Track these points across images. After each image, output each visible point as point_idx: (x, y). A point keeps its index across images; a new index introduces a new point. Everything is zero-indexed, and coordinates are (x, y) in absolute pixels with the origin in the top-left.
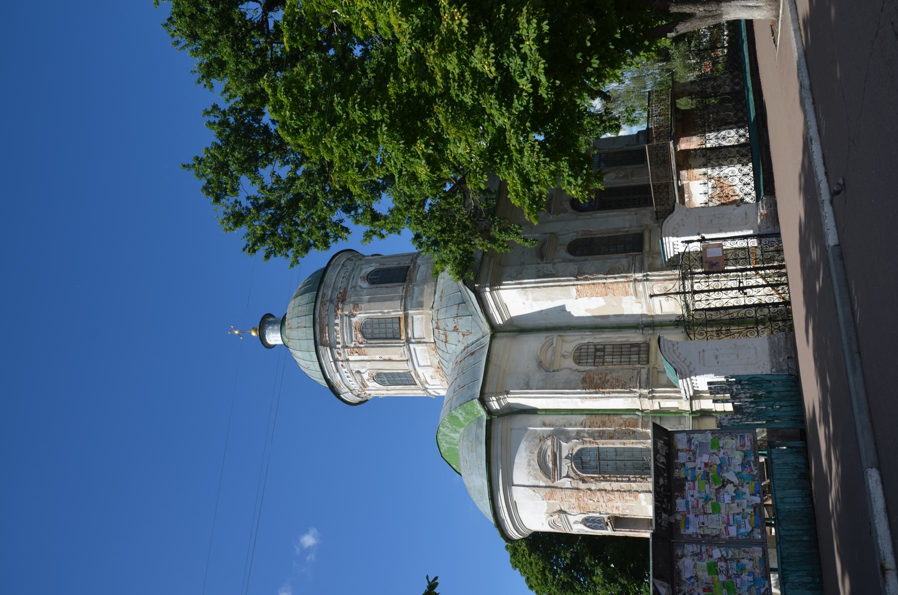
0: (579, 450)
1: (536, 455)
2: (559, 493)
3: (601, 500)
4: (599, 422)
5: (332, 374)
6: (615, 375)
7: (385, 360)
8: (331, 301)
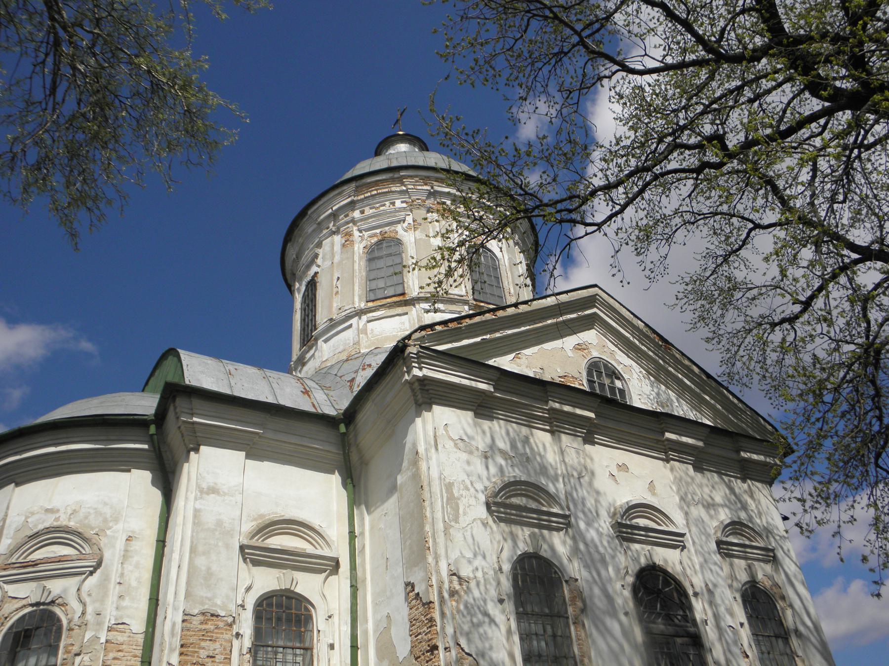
0: (59, 620)
1: (65, 523)
5: (315, 216)
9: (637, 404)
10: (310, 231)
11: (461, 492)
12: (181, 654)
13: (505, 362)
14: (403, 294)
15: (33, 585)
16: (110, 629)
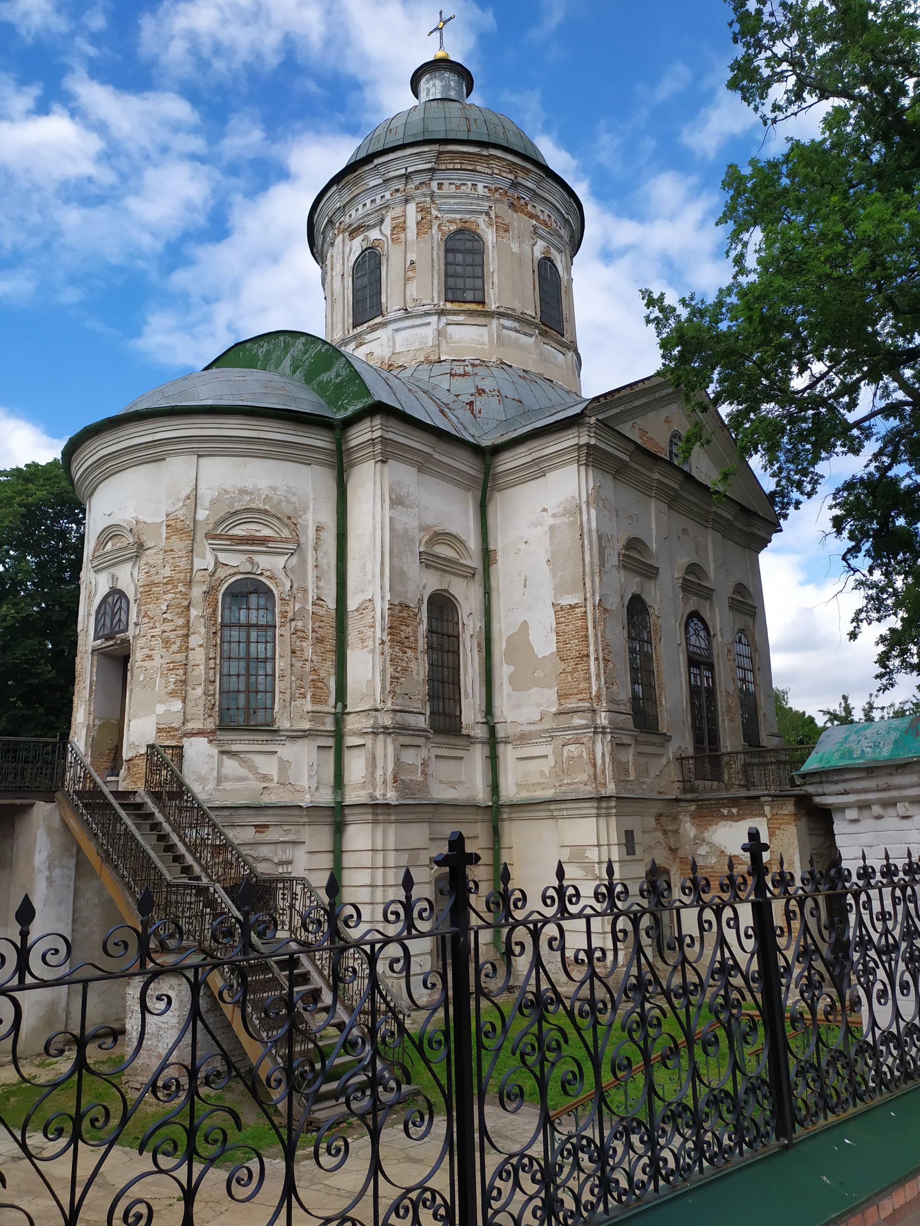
1: (261, 506)
2: (182, 545)
3: (168, 627)
5: (382, 169)
6: (413, 665)
8: (515, 185)
10: (372, 184)
12: (389, 634)
14: (483, 303)
15: (244, 557)
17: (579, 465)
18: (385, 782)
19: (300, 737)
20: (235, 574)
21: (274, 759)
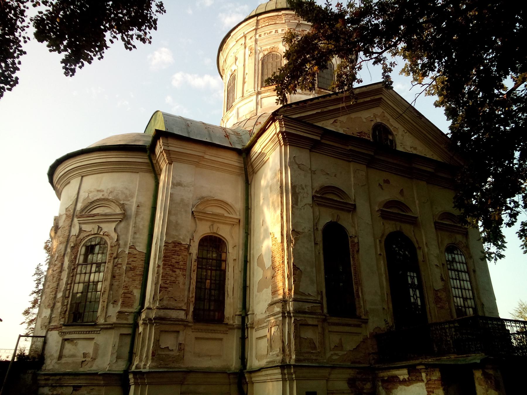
1: (107, 197)
4: (134, 264)
5: (234, 37)
6: (181, 279)
7: (244, 78)
9: (399, 148)
11: (300, 190)
13: (328, 125)
16: (130, 248)
17: (281, 147)
18: (147, 356)
19: (110, 328)
20: (89, 236)
21: (92, 343)
